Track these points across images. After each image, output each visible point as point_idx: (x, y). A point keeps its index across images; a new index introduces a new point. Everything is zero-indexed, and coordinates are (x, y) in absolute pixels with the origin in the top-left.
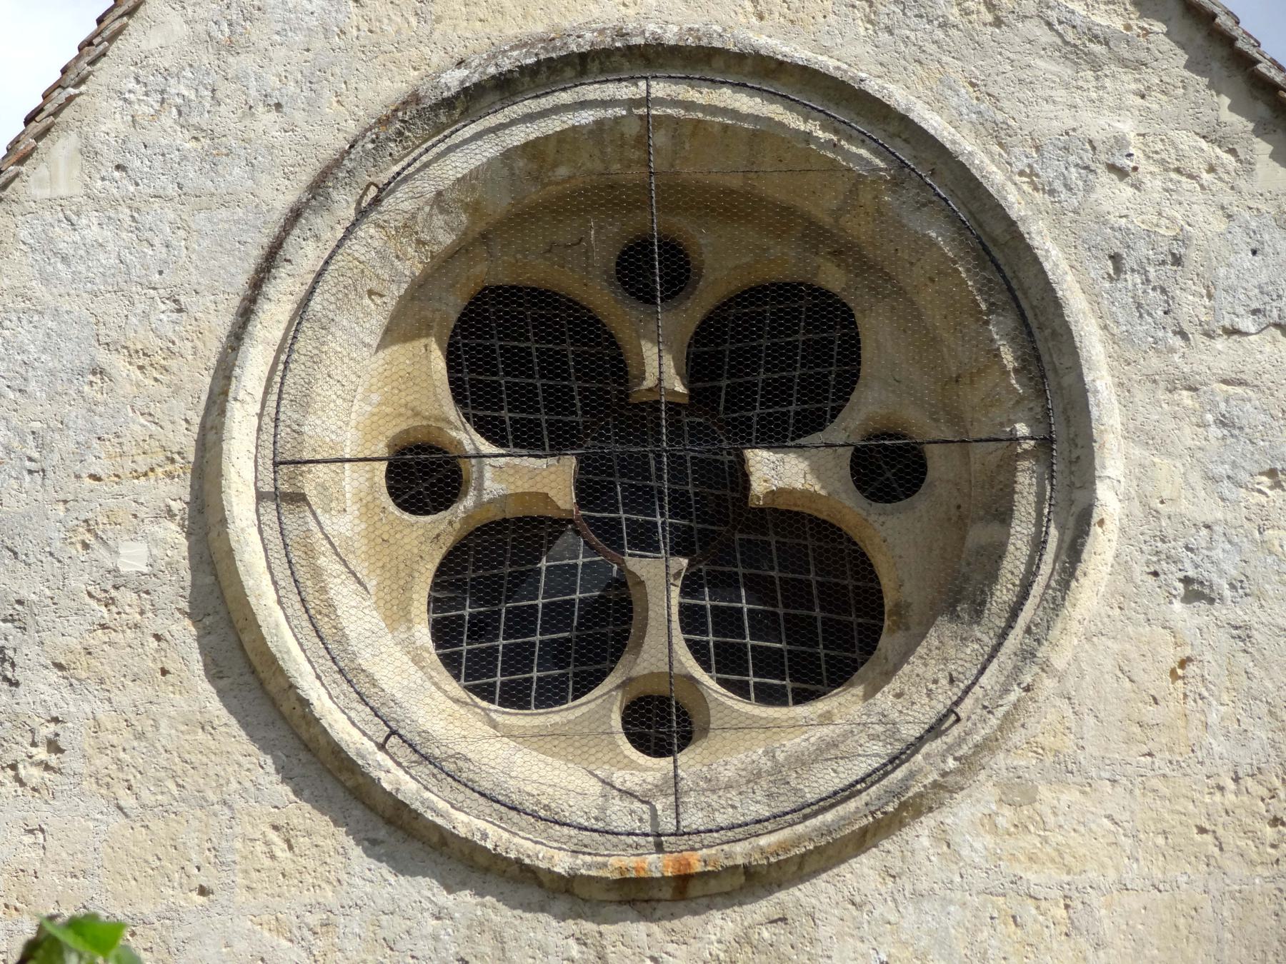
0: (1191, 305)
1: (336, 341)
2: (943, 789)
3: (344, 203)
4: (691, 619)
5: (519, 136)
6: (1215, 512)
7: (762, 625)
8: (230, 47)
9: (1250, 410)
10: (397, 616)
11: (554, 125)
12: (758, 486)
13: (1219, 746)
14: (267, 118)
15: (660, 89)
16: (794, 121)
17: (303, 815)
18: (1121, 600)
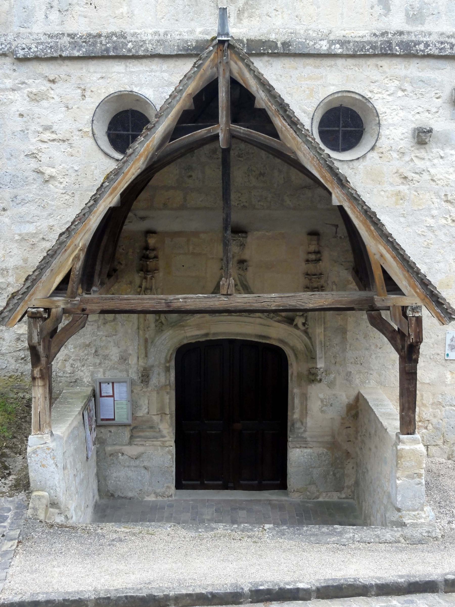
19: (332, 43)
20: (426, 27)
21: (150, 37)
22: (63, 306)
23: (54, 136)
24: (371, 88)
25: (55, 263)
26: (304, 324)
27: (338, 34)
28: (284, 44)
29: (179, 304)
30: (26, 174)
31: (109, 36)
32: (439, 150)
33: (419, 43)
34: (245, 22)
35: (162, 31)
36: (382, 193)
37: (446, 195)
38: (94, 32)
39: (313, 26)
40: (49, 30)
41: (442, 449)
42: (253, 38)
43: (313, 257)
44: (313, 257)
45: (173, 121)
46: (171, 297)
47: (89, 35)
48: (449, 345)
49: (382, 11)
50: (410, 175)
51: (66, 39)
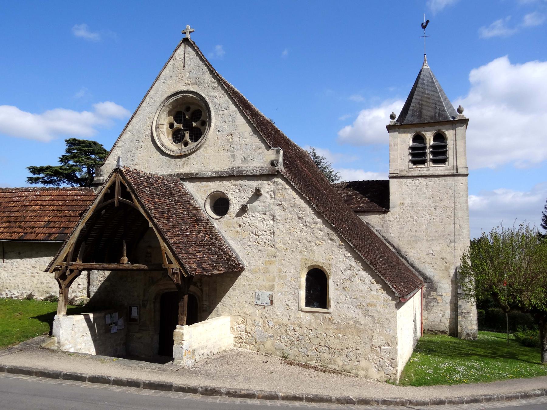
0: (220, 108)
1: (162, 116)
3: (162, 105)
4: (190, 136)
5: (175, 99)
6: (221, 125)
8: (156, 94)
10: (168, 137)
11: (177, 98)
12: (193, 125)
13: (219, 144)
14: (158, 99)
15: (184, 94)
16: (194, 96)
20: (249, 164)
22: (65, 265)
24: (227, 189)
26: (201, 286)
27: (216, 169)
28: (196, 174)
29: (106, 267)
32: (252, 213)
34: (185, 167)
36: (231, 231)
37: (255, 232)
41: (255, 346)
42: (186, 173)
45: (102, 197)
48: (257, 298)
49: (233, 160)
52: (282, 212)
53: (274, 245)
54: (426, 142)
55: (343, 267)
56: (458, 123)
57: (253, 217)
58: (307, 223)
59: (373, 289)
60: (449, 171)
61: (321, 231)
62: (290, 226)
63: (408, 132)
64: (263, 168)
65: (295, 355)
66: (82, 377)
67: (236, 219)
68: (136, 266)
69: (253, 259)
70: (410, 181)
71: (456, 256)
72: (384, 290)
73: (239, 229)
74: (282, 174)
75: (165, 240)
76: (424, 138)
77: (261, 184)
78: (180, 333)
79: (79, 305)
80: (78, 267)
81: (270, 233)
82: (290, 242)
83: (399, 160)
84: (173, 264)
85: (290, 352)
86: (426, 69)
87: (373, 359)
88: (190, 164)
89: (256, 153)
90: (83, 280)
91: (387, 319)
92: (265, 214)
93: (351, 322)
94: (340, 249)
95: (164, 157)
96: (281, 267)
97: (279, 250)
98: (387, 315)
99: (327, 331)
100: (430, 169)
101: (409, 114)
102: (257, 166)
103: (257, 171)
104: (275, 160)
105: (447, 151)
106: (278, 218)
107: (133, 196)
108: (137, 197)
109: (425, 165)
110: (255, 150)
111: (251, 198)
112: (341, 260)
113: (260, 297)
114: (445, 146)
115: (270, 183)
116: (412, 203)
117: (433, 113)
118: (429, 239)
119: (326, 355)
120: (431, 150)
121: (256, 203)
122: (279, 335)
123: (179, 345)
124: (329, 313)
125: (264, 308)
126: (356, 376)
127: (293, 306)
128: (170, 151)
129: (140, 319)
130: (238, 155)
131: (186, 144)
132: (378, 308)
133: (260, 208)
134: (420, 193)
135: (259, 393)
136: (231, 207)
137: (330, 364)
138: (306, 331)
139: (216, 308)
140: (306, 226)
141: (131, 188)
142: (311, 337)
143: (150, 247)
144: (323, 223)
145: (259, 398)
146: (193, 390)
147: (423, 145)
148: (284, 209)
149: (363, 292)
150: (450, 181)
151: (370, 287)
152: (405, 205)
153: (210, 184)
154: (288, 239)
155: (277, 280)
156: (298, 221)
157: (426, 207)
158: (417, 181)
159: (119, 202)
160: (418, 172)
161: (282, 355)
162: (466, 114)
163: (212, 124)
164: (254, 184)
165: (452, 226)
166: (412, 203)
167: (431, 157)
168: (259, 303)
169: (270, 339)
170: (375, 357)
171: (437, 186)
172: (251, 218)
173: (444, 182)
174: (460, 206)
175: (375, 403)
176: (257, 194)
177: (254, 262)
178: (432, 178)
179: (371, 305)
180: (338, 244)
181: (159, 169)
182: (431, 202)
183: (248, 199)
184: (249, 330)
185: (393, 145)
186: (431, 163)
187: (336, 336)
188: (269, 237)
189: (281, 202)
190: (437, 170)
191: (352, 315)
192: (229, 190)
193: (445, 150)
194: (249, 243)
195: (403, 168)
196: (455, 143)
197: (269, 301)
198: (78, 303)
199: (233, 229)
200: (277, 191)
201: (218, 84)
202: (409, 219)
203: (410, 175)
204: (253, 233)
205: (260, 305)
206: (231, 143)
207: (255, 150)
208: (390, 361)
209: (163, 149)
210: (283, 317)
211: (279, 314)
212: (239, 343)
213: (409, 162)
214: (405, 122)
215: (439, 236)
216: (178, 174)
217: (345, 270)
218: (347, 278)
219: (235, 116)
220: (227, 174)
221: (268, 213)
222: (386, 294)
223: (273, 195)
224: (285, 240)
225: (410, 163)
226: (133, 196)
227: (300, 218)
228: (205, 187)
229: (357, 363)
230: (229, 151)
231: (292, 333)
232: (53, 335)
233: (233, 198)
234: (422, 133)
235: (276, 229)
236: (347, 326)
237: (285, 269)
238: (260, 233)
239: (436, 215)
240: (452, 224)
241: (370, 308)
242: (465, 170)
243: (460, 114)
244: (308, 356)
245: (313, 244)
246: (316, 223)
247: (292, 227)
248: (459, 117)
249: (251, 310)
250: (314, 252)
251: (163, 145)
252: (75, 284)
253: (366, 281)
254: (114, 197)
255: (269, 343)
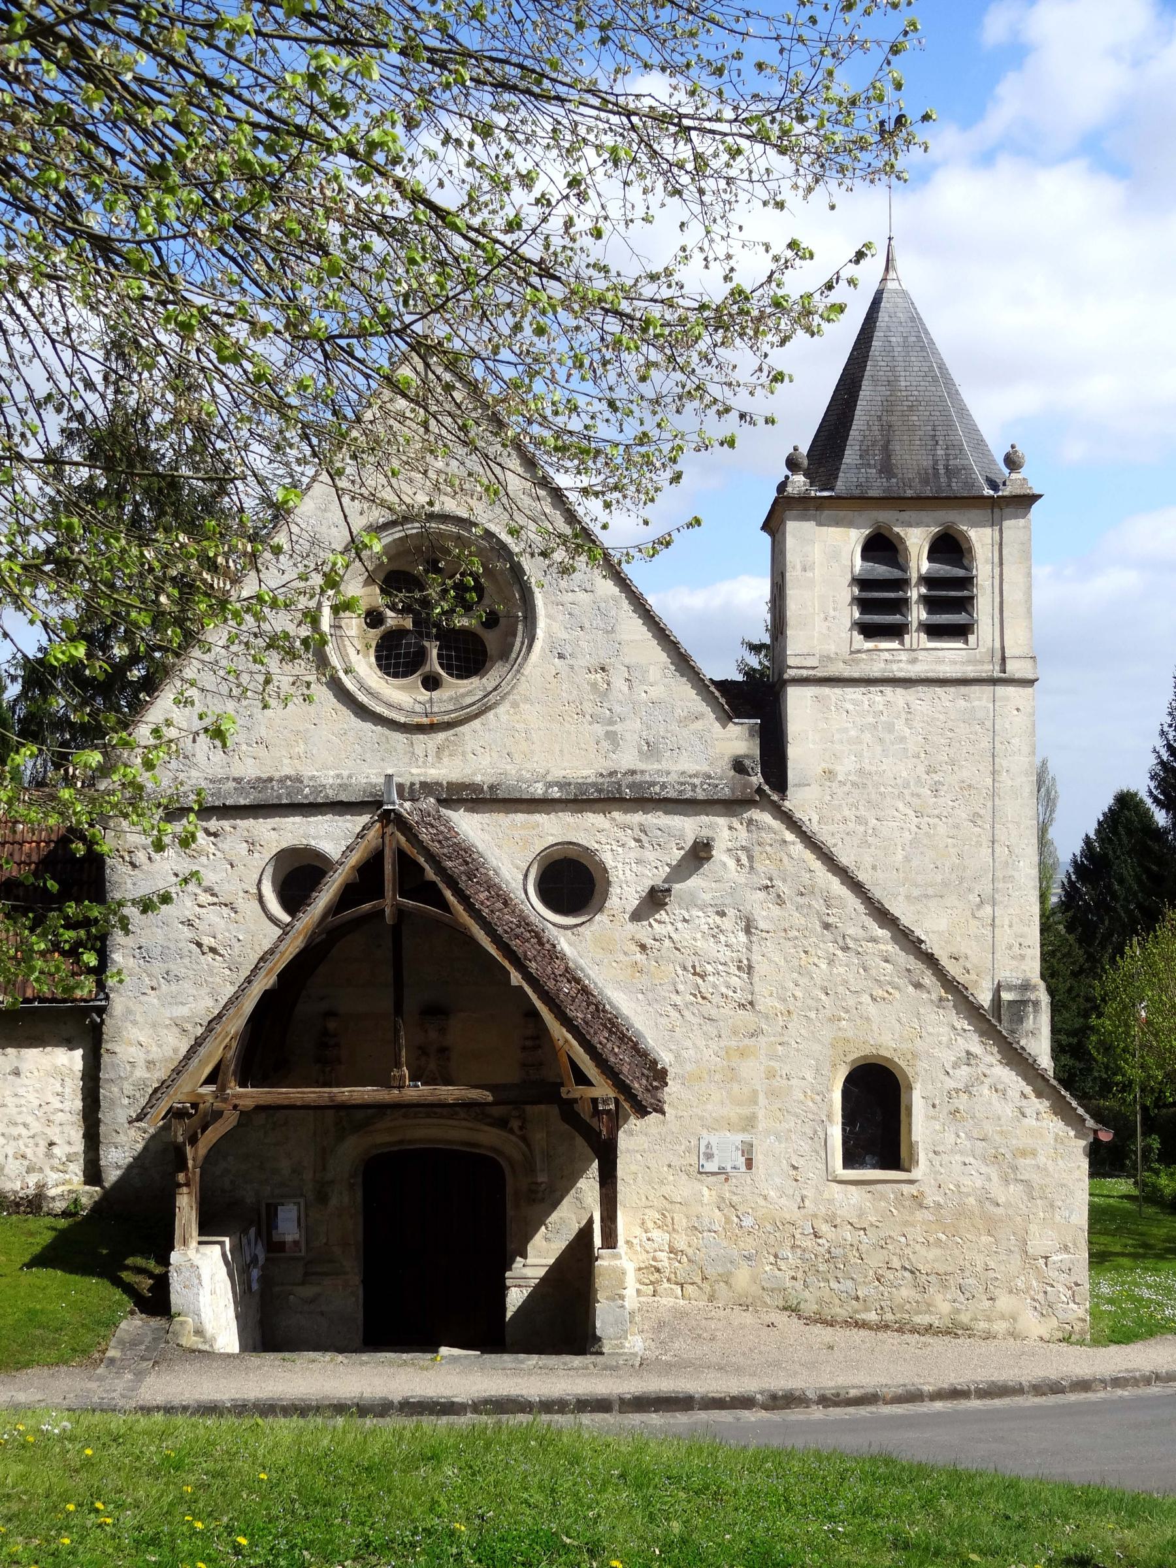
2: (496, 704)
4: (440, 656)
6: (566, 636)
7: (458, 658)
9: (576, 610)
14: (334, 529)
17: (339, 706)
18: (543, 657)
19: (549, 785)
20: (664, 765)
21: (331, 781)
23: (215, 900)
25: (202, 1051)
26: (521, 1128)
27: (557, 774)
28: (491, 787)
30: (180, 945)
31: (282, 781)
33: (654, 784)
34: (445, 760)
35: (345, 773)
37: (694, 967)
38: (264, 776)
39: (528, 766)
40: (210, 772)
43: (529, 1043)
44: (529, 1043)
46: (335, 1090)
47: (259, 779)
50: (649, 942)
51: (233, 784)
52: (776, 911)
53: (751, 1003)
54: (907, 561)
55: (948, 1057)
56: (1007, 506)
57: (685, 920)
58: (848, 940)
59: (1028, 1111)
60: (979, 668)
61: (887, 961)
62: (800, 950)
63: (850, 524)
64: (710, 777)
65: (820, 1301)
66: (453, 1403)
67: (632, 927)
68: (448, 1093)
69: (688, 1043)
70: (854, 696)
71: (998, 948)
72: (1056, 1114)
73: (640, 957)
74: (773, 802)
75: (567, 1022)
76: (900, 547)
77: (710, 826)
78: (614, 1269)
79: (65, 1214)
80: (237, 1102)
81: (739, 968)
82: (799, 994)
83: (818, 619)
84: (592, 1085)
85: (807, 1293)
86: (895, 291)
87: (1029, 1288)
88: (464, 754)
89: (685, 732)
90: (67, 1128)
91: (1062, 1186)
92: (722, 914)
93: (971, 1200)
94: (941, 1011)
95: (368, 726)
96: (772, 1063)
97: (767, 1017)
98: (1064, 1175)
99: (908, 1230)
100: (921, 655)
101: (850, 456)
102: (691, 772)
103: (694, 786)
104: (747, 756)
105: (971, 599)
106: (762, 925)
107: (448, 894)
108: (464, 899)
109: (902, 643)
110: (683, 722)
111: (679, 865)
112: (944, 1039)
113: (715, 1151)
114: (967, 582)
115: (735, 823)
116: (861, 771)
117: (927, 463)
118: (916, 892)
119: (906, 1293)
120: (923, 590)
121: (694, 882)
122: (772, 1251)
123: (614, 1300)
124: (912, 1182)
125: (727, 1180)
126: (988, 1336)
127: (812, 1171)
128: (389, 705)
129: (307, 1243)
130: (628, 736)
131: (431, 683)
132: (1042, 1160)
133: (707, 897)
134: (888, 737)
135: (885, 1390)
136: (614, 890)
137: (918, 1313)
138: (848, 1234)
139: (573, 1192)
140: (845, 949)
141: (441, 870)
142: (863, 1248)
143: (330, 1014)
144: (894, 939)
145: (886, 1402)
146: (744, 1402)
147: (895, 574)
148: (780, 901)
149: (1003, 1121)
150: (980, 699)
151: (1020, 1108)
152: (840, 778)
153: (540, 818)
154: (792, 985)
155: (762, 1098)
156: (823, 935)
157: (906, 785)
158: (878, 697)
159: (400, 912)
160: (882, 665)
161: (781, 1303)
162: (1030, 478)
163: (540, 633)
164: (689, 827)
165: (986, 851)
166: (861, 771)
167: (924, 616)
168: (711, 1167)
169: (744, 1263)
170: (1035, 1283)
171: (942, 717)
172: (680, 925)
173: (962, 703)
174: (1010, 783)
175: (1100, 1386)
176: (700, 853)
177: (691, 1052)
178: (926, 689)
179: (1024, 1153)
180: (934, 997)
181: (350, 763)
182: (921, 769)
183: (668, 869)
184: (681, 1243)
185: (799, 567)
186: (923, 636)
187: (931, 1240)
188: (734, 981)
189: (771, 880)
190: (940, 661)
191: (973, 1181)
192: (604, 841)
193: (966, 593)
194: (674, 997)
195: (831, 648)
196: (997, 570)
197: (741, 1162)
198: (59, 1206)
199: (622, 957)
200: (757, 848)
201: (554, 506)
202: (851, 825)
203: (856, 675)
204: (685, 969)
205: (713, 1174)
206: (605, 694)
207: (683, 722)
208: (1070, 1288)
209: (362, 698)
210: (783, 1201)
211: (772, 1193)
212: (652, 1283)
213: (851, 629)
214: (842, 485)
215: (945, 884)
216: (424, 785)
217: (955, 1066)
218: (961, 1086)
219: (613, 613)
220: (600, 791)
221: (731, 912)
222: (1061, 1124)
223: (744, 860)
224: (783, 988)
225: (855, 633)
226: (448, 894)
227: (827, 926)
228: (523, 827)
229: (988, 1303)
230: (595, 719)
231: (808, 1243)
232: (173, 1310)
233: (620, 865)
234: (896, 529)
235: (756, 957)
236: (962, 1212)
237: (786, 1069)
238: (709, 968)
239: (936, 812)
240: (986, 843)
241: (1022, 1162)
242: (1028, 664)
243: (1014, 476)
244: (857, 1298)
245: (866, 998)
246: (874, 940)
247: (806, 952)
248: (1014, 484)
249: (684, 1188)
250: (868, 1019)
251: (362, 686)
252: (37, 1145)
253: (1010, 1093)
254: (380, 894)
255: (742, 1277)
